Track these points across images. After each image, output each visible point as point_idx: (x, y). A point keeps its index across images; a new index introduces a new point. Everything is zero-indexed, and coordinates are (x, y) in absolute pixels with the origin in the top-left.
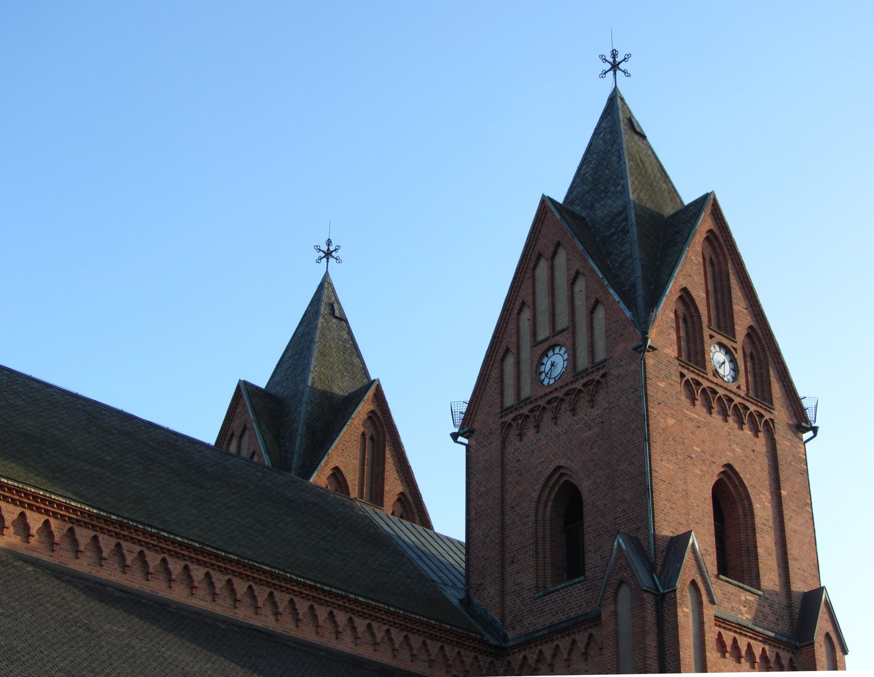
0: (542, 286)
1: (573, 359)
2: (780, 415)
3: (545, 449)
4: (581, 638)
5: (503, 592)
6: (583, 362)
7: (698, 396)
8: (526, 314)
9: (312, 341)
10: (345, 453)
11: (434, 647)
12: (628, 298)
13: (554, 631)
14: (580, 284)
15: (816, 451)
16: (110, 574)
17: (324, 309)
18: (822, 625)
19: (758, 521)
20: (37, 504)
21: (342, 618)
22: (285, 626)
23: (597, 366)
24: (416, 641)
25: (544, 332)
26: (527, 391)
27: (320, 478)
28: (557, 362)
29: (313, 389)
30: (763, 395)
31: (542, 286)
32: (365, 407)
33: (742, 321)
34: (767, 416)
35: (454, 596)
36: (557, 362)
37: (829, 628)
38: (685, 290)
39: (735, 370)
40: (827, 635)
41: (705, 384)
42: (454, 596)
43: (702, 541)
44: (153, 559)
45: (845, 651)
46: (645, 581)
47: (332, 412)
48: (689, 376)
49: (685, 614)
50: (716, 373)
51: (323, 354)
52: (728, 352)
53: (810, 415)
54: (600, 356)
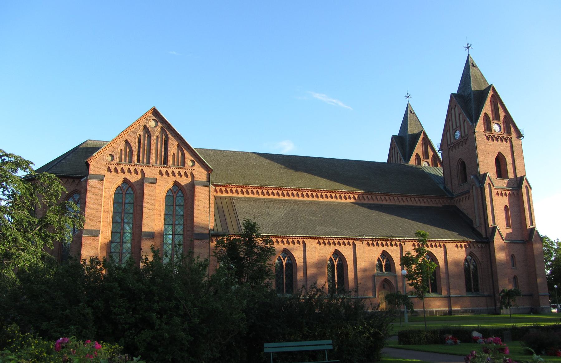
0: (453, 115)
1: (461, 134)
2: (514, 135)
3: (458, 154)
4: (467, 196)
5: (452, 185)
6: (463, 135)
7: (490, 139)
8: (450, 122)
9: (407, 122)
10: (418, 149)
11: (437, 200)
12: (471, 120)
13: (462, 194)
14: (461, 116)
15: (524, 141)
16: (371, 202)
17: (409, 112)
18: (525, 184)
19: (508, 163)
20: (355, 193)
21: (417, 199)
22: (406, 203)
23: (466, 136)
24: (433, 200)
25: (454, 127)
26: (452, 141)
27: (412, 162)
28: (458, 134)
29: (409, 134)
30: (509, 132)
31: (453, 115)
32: (422, 137)
33: (502, 114)
34: (510, 137)
35: (442, 187)
36: (458, 134)
37: (527, 184)
38: (485, 113)
39: (500, 128)
40: (526, 186)
41: (492, 135)
42: (442, 187)
43: (492, 173)
44: (378, 197)
45: (531, 189)
46: (477, 184)
47: (415, 138)
48: (487, 134)
49: (487, 191)
50: (495, 131)
51: (410, 124)
52: (498, 124)
53: (522, 133)
54: (466, 133)
